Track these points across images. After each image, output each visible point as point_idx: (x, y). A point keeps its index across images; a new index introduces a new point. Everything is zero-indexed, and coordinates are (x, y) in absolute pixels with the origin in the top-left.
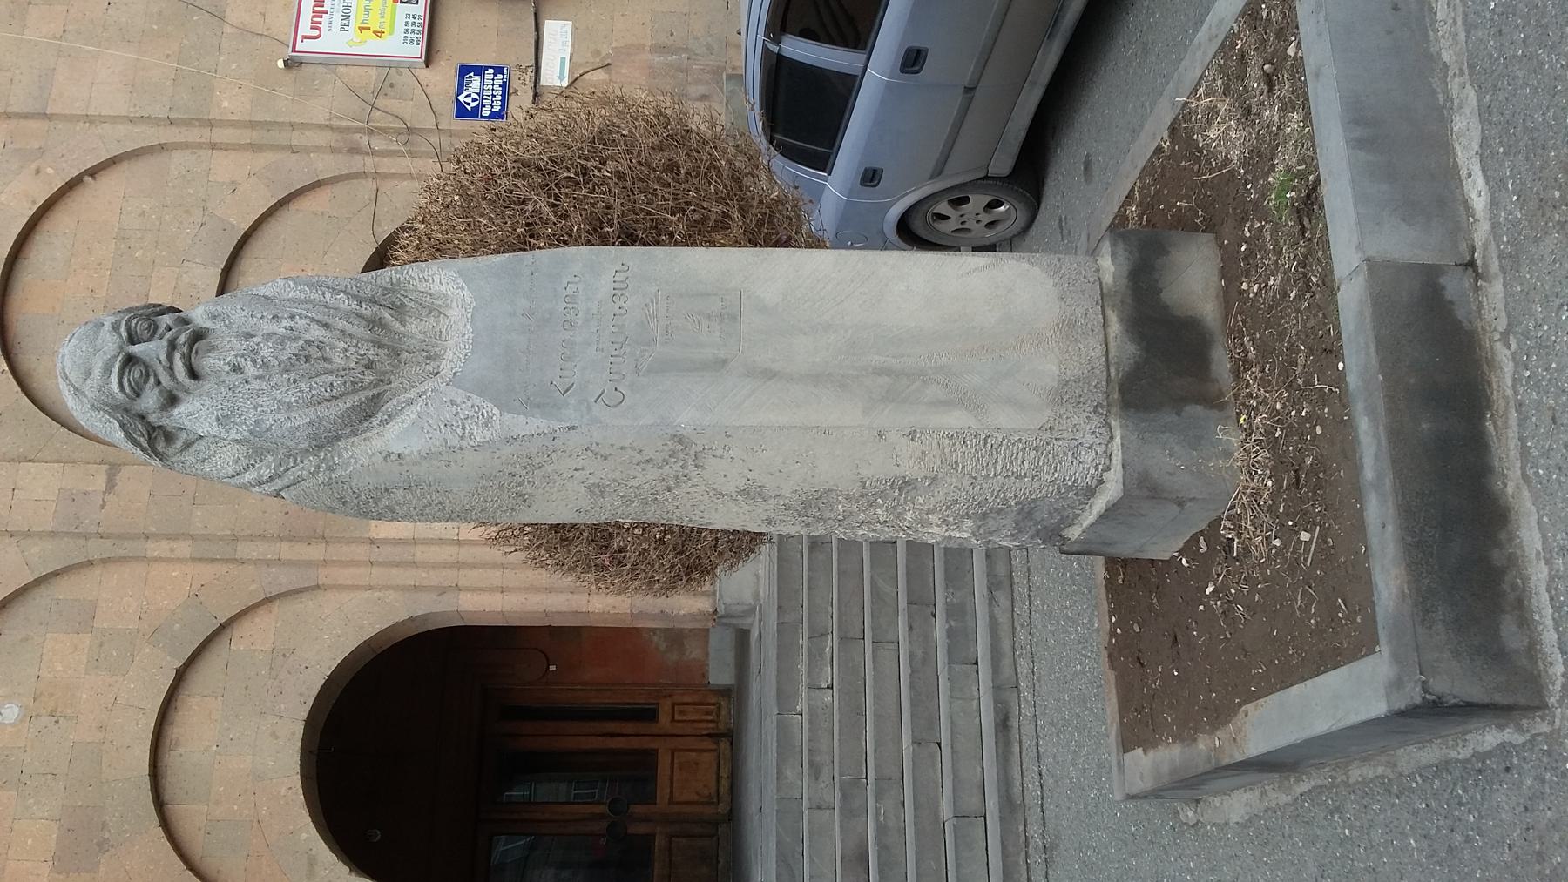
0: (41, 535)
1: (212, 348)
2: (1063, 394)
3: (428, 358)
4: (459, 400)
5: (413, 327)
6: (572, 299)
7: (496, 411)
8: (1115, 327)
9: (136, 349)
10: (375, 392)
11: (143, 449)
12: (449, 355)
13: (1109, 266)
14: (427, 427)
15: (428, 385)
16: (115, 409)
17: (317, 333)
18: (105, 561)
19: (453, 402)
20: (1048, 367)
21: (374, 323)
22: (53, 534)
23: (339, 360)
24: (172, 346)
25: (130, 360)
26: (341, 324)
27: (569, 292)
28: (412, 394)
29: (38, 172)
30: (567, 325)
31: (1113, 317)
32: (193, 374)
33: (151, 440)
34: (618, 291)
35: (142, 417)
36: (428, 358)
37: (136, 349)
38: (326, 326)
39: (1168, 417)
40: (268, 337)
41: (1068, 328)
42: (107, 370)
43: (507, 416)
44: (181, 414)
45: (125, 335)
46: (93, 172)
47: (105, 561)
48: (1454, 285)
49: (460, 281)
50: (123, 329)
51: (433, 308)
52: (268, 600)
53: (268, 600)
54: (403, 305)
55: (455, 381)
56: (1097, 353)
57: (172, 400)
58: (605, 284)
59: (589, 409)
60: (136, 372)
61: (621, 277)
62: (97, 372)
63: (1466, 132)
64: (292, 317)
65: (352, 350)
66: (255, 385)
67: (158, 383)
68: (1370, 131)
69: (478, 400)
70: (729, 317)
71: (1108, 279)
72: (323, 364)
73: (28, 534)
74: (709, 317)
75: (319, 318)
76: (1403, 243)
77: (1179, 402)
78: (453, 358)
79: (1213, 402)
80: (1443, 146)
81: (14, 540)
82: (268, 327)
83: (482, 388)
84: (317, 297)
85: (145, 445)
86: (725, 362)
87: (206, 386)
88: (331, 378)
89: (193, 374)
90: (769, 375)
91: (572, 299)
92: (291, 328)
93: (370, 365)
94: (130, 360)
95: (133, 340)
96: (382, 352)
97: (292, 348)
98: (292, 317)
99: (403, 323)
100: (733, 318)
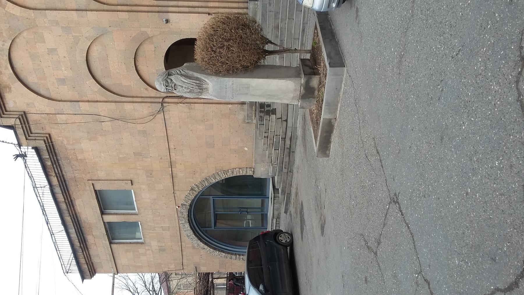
2: (293, 98)
5: (204, 86)
6: (226, 85)
8: (302, 89)
13: (303, 81)
20: (292, 95)
31: (302, 87)
39: (307, 100)
41: (295, 90)
48: (332, 121)
56: (299, 93)
58: (231, 83)
63: (339, 105)
68: (328, 104)
70: (248, 88)
71: (302, 82)
76: (328, 116)
77: (309, 98)
79: (314, 98)
80: (337, 106)
90: (254, 95)
91: (226, 85)
100: (249, 88)
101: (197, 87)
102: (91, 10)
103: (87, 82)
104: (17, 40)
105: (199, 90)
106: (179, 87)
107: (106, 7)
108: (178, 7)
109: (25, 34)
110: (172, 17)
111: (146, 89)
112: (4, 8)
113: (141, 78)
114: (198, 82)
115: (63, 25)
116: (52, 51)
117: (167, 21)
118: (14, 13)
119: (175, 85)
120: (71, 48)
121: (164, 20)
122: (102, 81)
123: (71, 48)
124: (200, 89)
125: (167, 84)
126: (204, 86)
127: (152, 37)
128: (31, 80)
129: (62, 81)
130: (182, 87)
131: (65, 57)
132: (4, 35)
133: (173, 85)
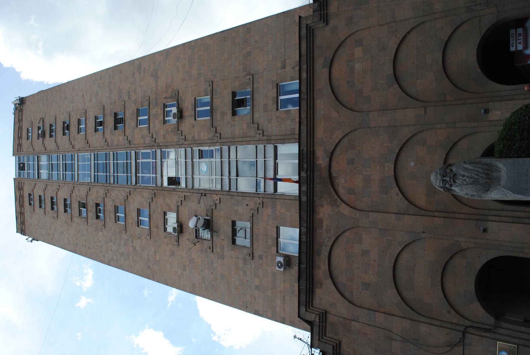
1: (457, 178)
5: (494, 174)
9: (444, 178)
12: (502, 181)
16: (441, 187)
18: (427, 130)
21: (487, 174)
23: (481, 181)
24: (450, 178)
25: (443, 180)
29: (396, 36)
32: (455, 182)
35: (446, 188)
37: (444, 178)
38: (478, 175)
40: (467, 177)
42: (440, 182)
43: (515, 195)
44: (452, 188)
46: (408, 33)
47: (427, 130)
51: (498, 170)
52: (465, 136)
53: (465, 136)
55: (504, 187)
57: (451, 186)
60: (445, 182)
62: (438, 182)
73: (410, 125)
78: (502, 183)
82: (466, 174)
83: (509, 189)
89: (455, 182)
94: (443, 180)
95: (444, 176)
97: (472, 180)
102: (409, 215)
103: (389, 292)
104: (340, 239)
106: (460, 177)
107: (423, 212)
108: (500, 216)
109: (347, 233)
110: (492, 226)
111: (449, 312)
112: (338, 208)
113: (445, 296)
114: (485, 167)
115: (381, 228)
116: (365, 253)
117: (485, 230)
118: (344, 213)
119: (455, 175)
120: (383, 252)
121: (481, 229)
122: (404, 293)
123: (383, 252)
124: (488, 178)
126: (494, 174)
128: (341, 279)
129: (366, 286)
130: (463, 176)
131: (375, 260)
133: (452, 176)
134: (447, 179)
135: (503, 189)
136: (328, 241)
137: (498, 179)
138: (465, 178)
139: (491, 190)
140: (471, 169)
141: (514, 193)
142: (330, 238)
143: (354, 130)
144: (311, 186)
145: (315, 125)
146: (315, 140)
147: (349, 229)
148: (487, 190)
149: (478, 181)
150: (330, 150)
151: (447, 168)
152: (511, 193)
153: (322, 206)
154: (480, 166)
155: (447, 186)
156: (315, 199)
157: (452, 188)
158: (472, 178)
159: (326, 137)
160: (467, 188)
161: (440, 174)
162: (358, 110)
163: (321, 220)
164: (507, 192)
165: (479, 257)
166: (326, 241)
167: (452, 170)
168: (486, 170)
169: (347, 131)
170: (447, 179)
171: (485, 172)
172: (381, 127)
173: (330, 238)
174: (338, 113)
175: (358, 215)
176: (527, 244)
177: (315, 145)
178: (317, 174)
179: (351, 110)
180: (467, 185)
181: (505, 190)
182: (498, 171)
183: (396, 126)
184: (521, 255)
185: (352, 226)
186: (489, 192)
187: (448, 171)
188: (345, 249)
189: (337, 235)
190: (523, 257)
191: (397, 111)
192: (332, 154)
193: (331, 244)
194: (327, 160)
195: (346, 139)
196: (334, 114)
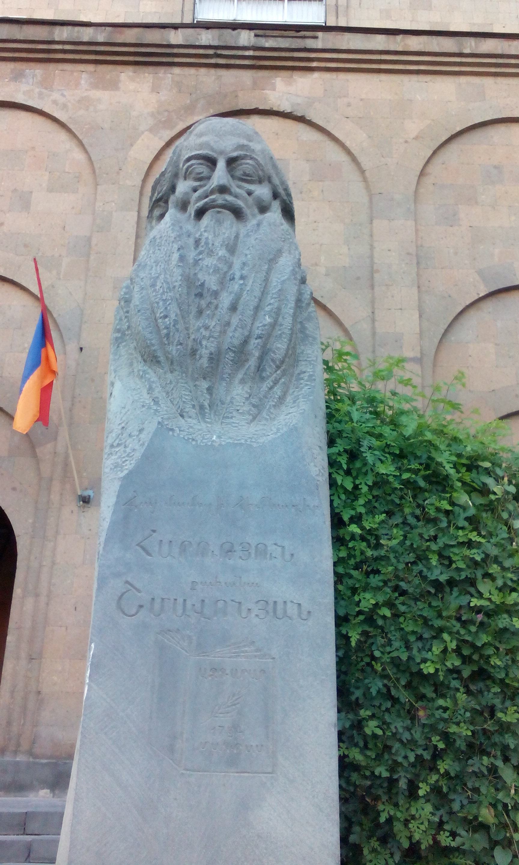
0: (373, 328)
3: (202, 407)
4: (142, 436)
5: (239, 391)
7: (126, 472)
9: (221, 164)
10: (162, 359)
11: (151, 198)
14: (124, 411)
15: (165, 407)
17: (226, 300)
19: (141, 431)
21: (241, 352)
22: (374, 334)
24: (223, 189)
25: (212, 162)
26: (235, 321)
27: (271, 548)
28: (158, 392)
30: (227, 547)
33: (158, 200)
34: (272, 608)
35: (173, 189)
36: (202, 407)
37: (221, 164)
38: (233, 308)
45: (235, 154)
49: (285, 429)
50: (242, 153)
54: (263, 379)
57: (184, 206)
58: (282, 590)
59: (118, 575)
60: (203, 169)
61: (292, 610)
64: (242, 278)
65: (206, 333)
66: (176, 256)
67: (195, 190)
69: (138, 455)
70: (234, 756)
72: (194, 310)
73: (373, 321)
74: (235, 728)
75: (242, 301)
81: (371, 314)
83: (151, 456)
84: (269, 299)
85: (154, 200)
86: (172, 749)
87: (189, 226)
88: (173, 316)
91: (262, 552)
92: (233, 279)
93: (194, 352)
94: (212, 162)
96: (204, 362)
98: (242, 278)
99: (243, 381)
100: (232, 762)
101: (234, 337)
104: (63, 135)
105: (207, 348)
109: (78, 155)
112: (151, 130)
114: (280, 347)
115: (94, 241)
116: (24, 201)
118: (135, 147)
120: (26, 246)
123: (26, 246)
124: (215, 359)
125: (247, 166)
126: (239, 391)
127: (34, 455)
130: (232, 249)
132: (81, 112)
134: (220, 174)
135: (151, 427)
136: (55, 102)
137: (210, 407)
138: (222, 252)
139: (152, 375)
140: (267, 280)
141: (128, 481)
142: (64, 107)
143: (365, 180)
144: (213, 61)
145: (384, 77)
146: (342, 76)
147: (90, 159)
148: (151, 359)
149: (200, 312)
150: (312, 116)
151: (276, 196)
152: (129, 466)
153: (155, 89)
154: (287, 322)
155: (183, 187)
156: (177, 70)
157: (172, 213)
158: (221, 283)
159: (349, 105)
160: (168, 262)
161: (241, 147)
162: (422, 190)
163: (114, 85)
164: (136, 448)
165: (14, 489)
166: (56, 96)
167: (263, 209)
168: (264, 353)
169: (362, 159)
170: (220, 174)
171: (254, 343)
172: (372, 247)
173: (64, 107)
174: (416, 138)
175: (129, 183)
176: (47, 604)
177: (327, 76)
178: (247, 76)
179: (422, 174)
180: (182, 258)
181: (145, 437)
182: (259, 407)
183: (372, 287)
184: (17, 591)
185: (97, 166)
186: (139, 366)
187: (263, 191)
188: (33, 148)
189: (71, 126)
190: (14, 595)
191: (415, 290)
192: (301, 119)
193: (46, 110)
194: (286, 107)
195: (343, 157)
196: (413, 127)
